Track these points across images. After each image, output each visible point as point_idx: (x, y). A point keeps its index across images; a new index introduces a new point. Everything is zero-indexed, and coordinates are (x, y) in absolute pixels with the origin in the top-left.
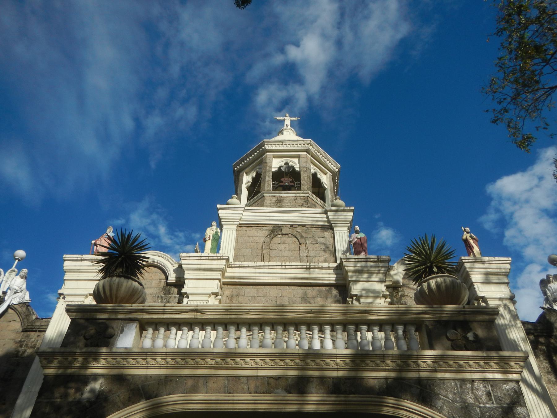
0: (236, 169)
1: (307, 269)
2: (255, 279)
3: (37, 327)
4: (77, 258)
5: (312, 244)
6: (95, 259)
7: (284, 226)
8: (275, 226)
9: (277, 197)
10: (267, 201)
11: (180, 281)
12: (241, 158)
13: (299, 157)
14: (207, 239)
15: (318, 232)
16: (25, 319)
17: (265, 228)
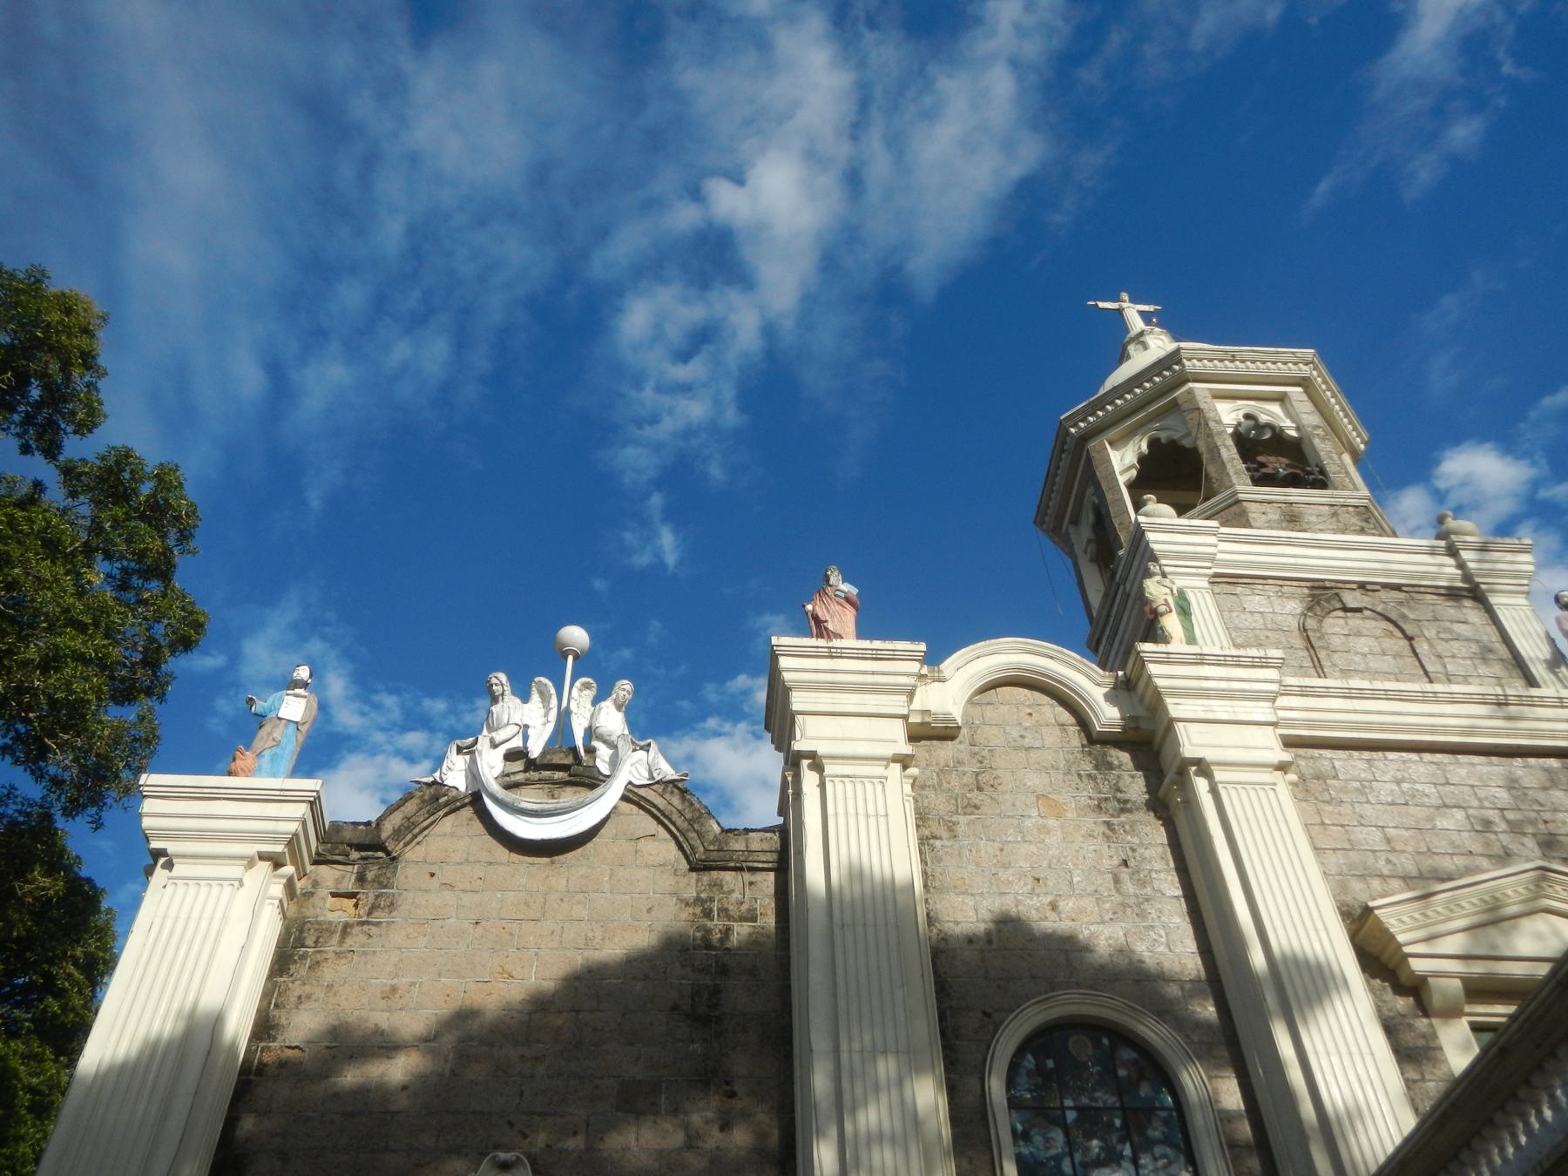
0: (1073, 430)
1: (1499, 704)
2: (1357, 729)
3: (738, 856)
4: (817, 647)
5: (1442, 639)
6: (874, 652)
7: (1340, 585)
8: (1316, 584)
9: (1280, 505)
10: (1254, 515)
11: (1137, 729)
12: (1091, 399)
13: (1281, 399)
14: (1162, 609)
15: (1448, 609)
16: (688, 830)
17: (1285, 589)
